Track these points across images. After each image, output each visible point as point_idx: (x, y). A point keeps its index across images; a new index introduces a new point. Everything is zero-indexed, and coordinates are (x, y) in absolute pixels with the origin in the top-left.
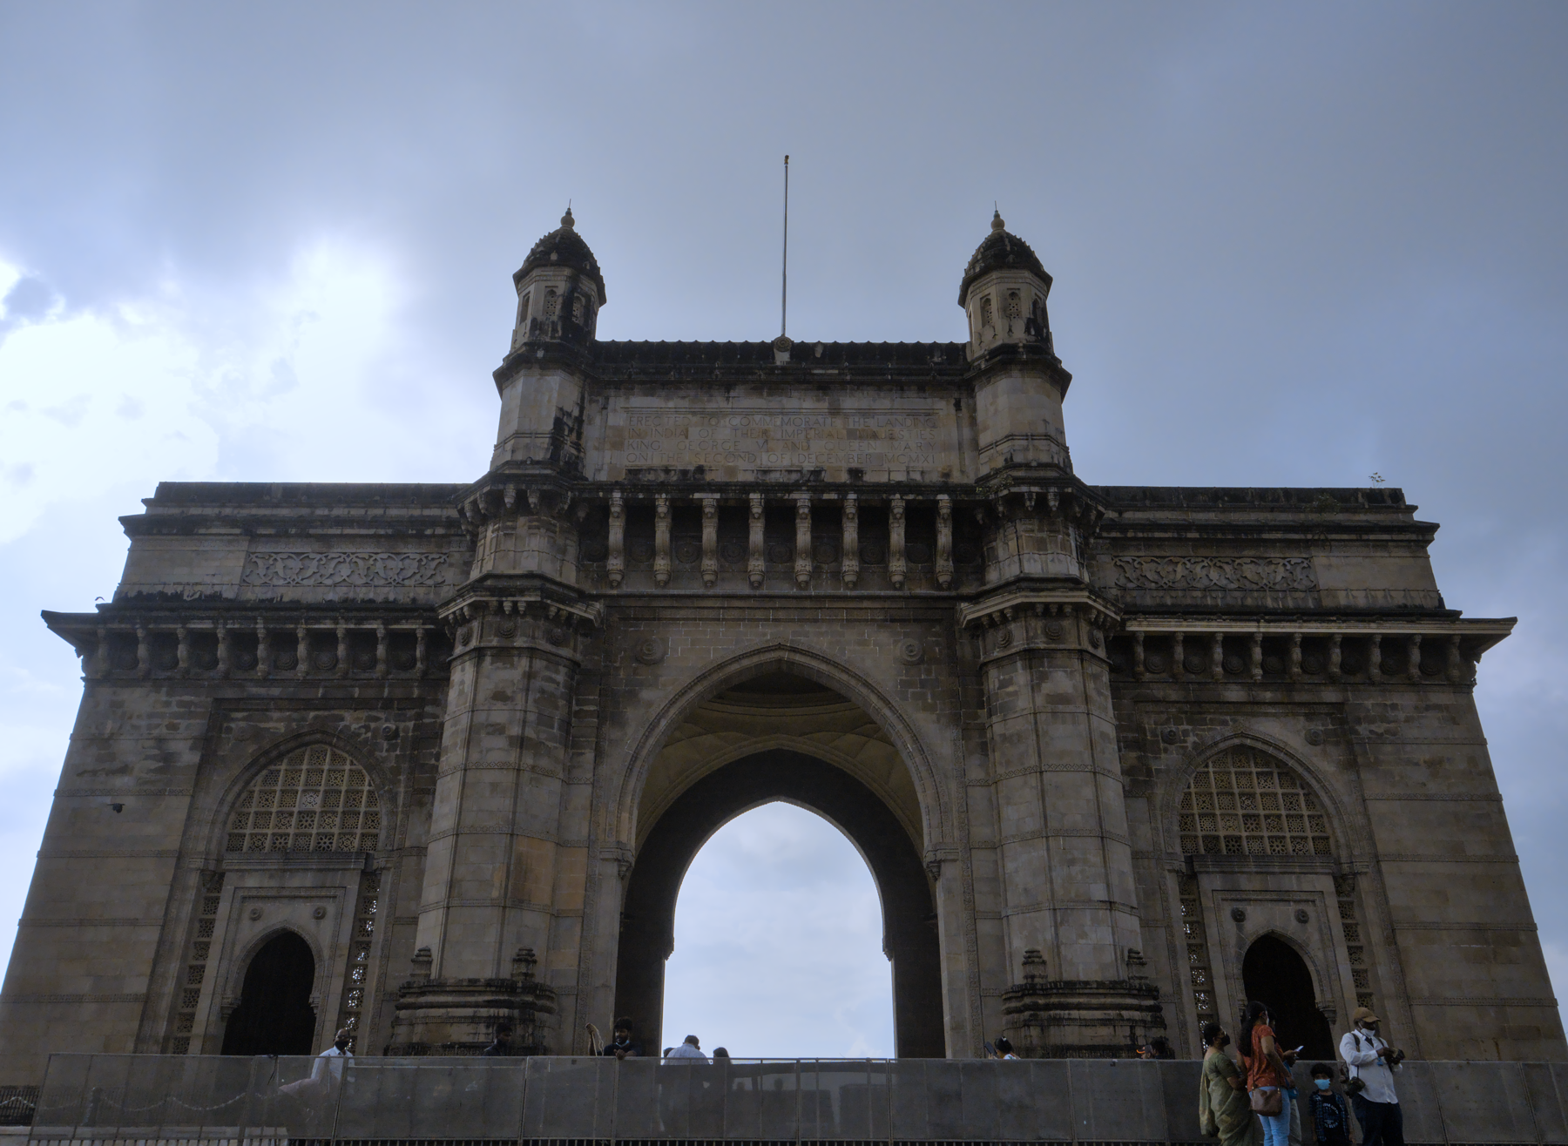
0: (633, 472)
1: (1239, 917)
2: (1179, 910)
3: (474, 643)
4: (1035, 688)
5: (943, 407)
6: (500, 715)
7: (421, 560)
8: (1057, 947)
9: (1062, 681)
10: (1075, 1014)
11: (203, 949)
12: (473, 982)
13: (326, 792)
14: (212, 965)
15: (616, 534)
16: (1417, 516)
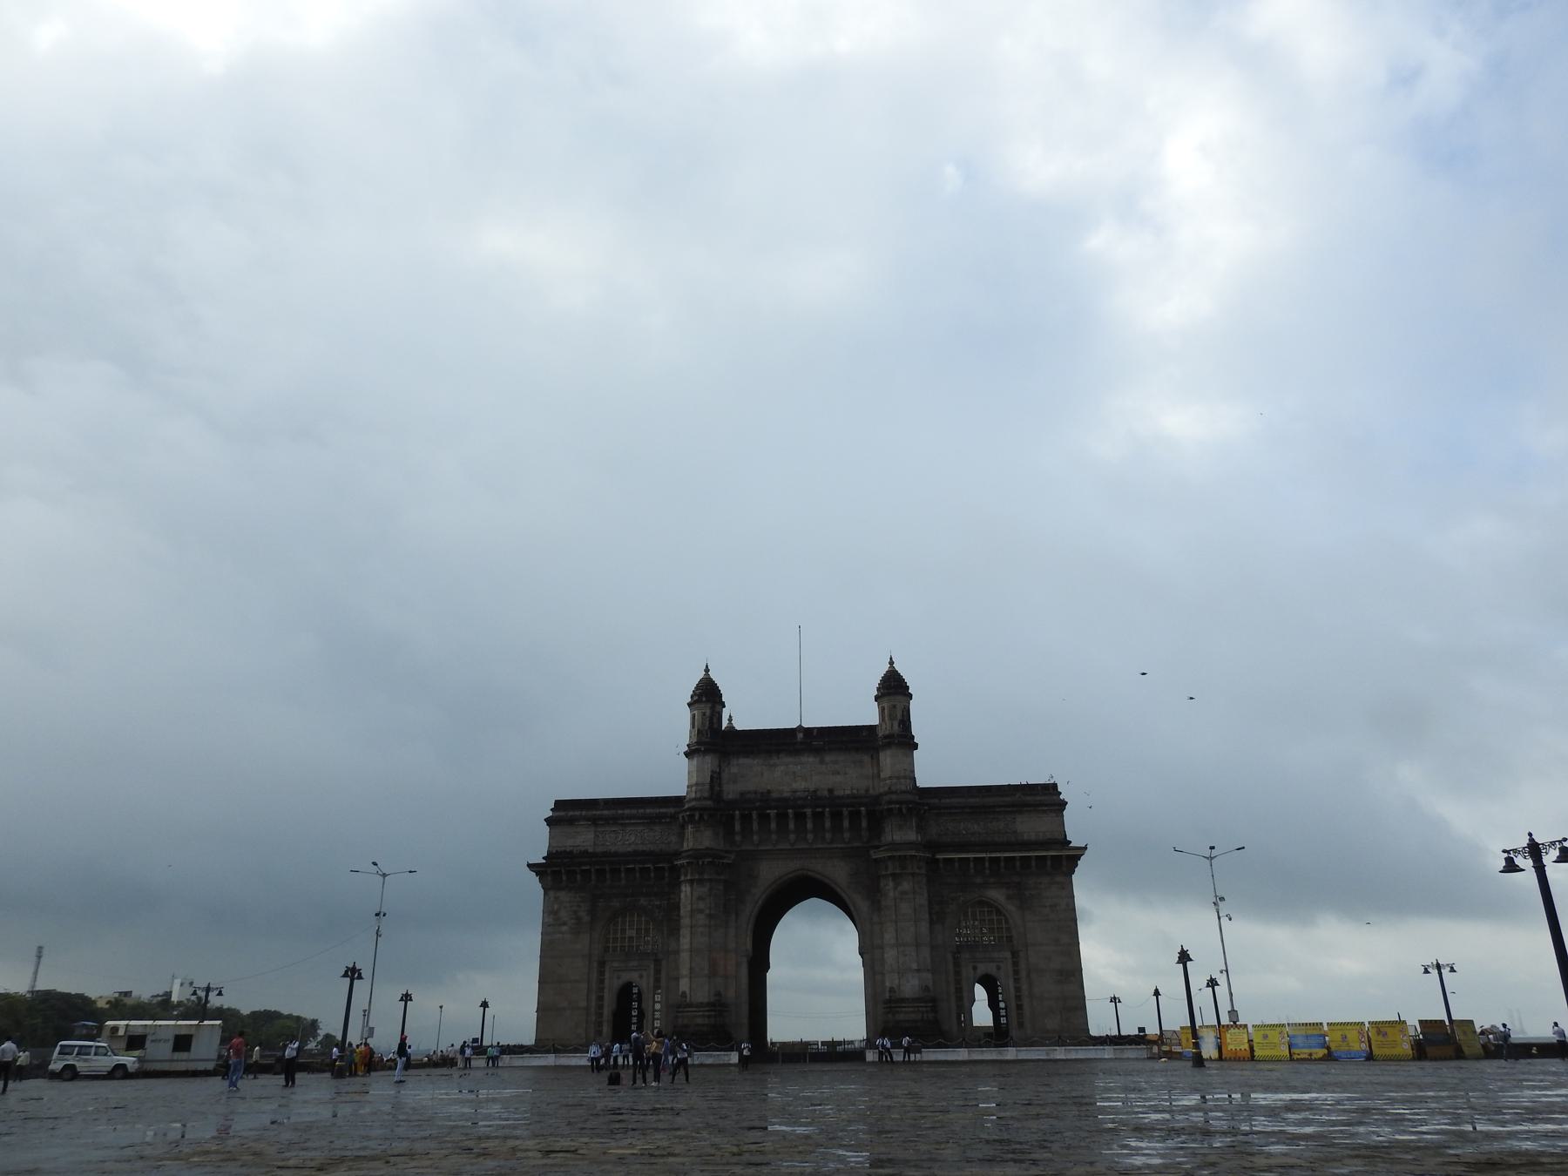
0: (742, 794)
1: (975, 968)
2: (951, 967)
3: (689, 878)
4: (895, 888)
5: (866, 758)
6: (701, 905)
8: (899, 986)
9: (906, 886)
10: (904, 1009)
11: (602, 989)
12: (702, 1003)
14: (606, 995)
15: (738, 827)
16: (1061, 797)
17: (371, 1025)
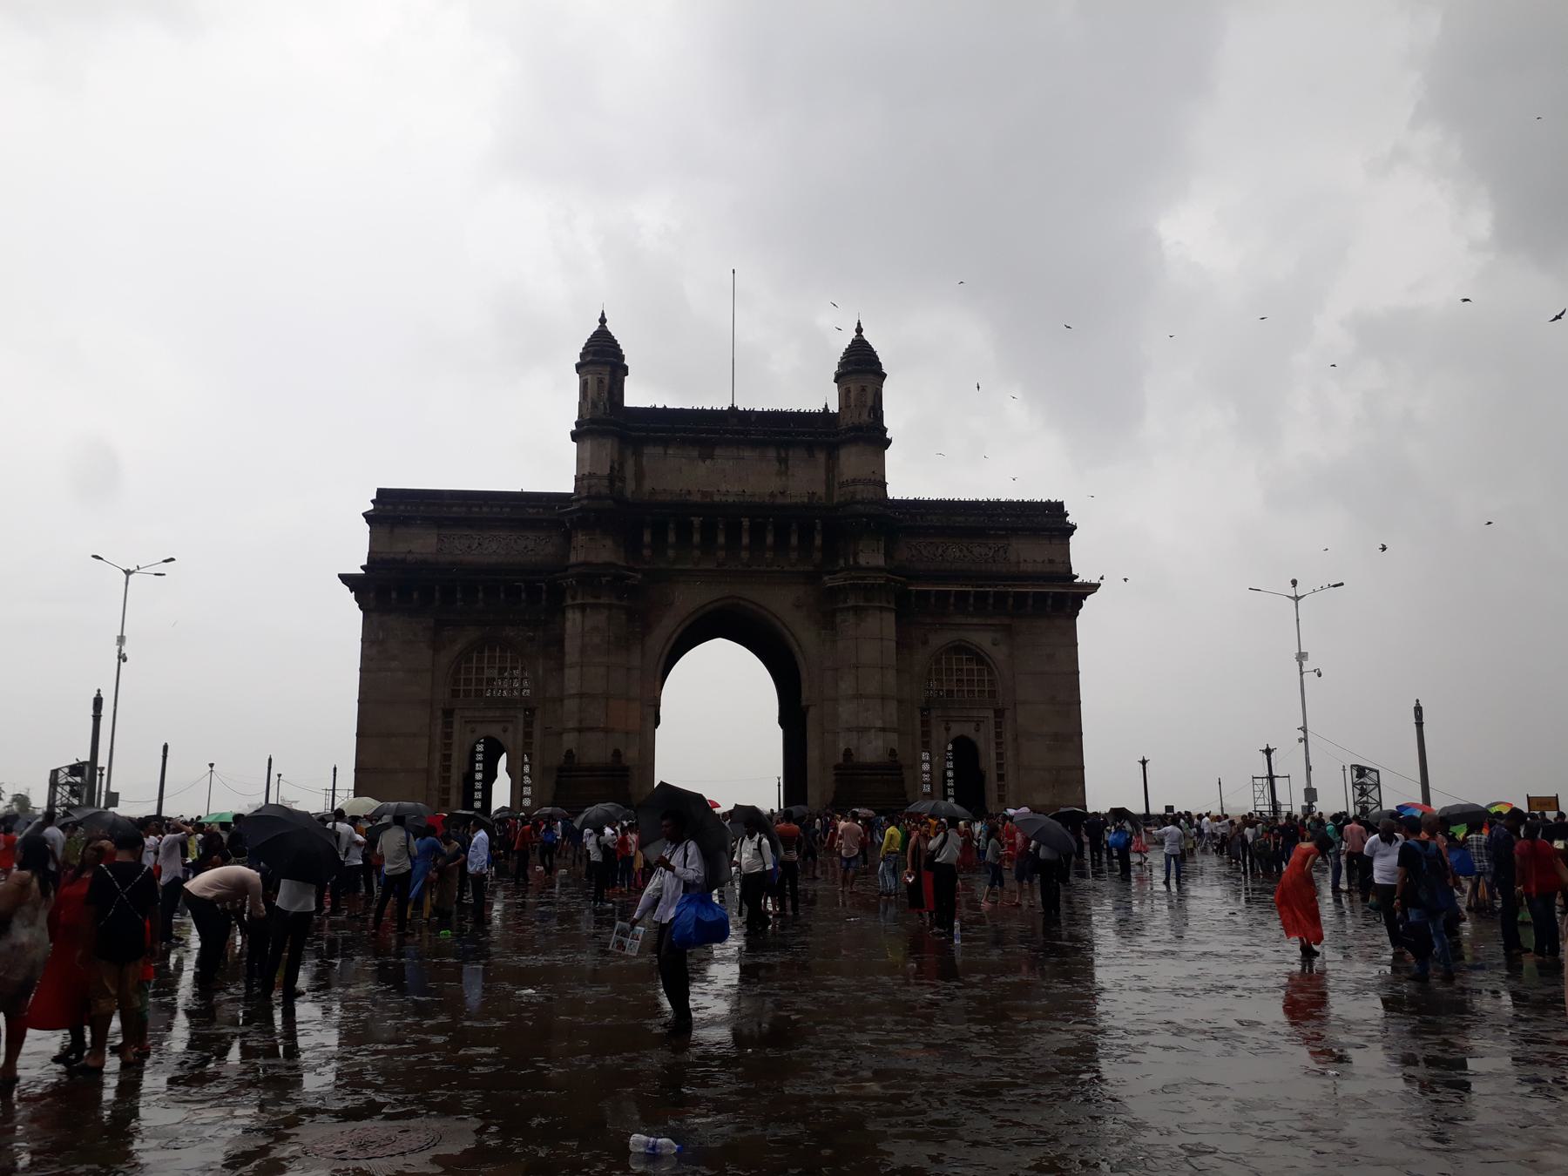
1: (948, 729)
3: (579, 601)
7: (536, 540)
11: (448, 746)
13: (499, 667)
17: (113, 790)
